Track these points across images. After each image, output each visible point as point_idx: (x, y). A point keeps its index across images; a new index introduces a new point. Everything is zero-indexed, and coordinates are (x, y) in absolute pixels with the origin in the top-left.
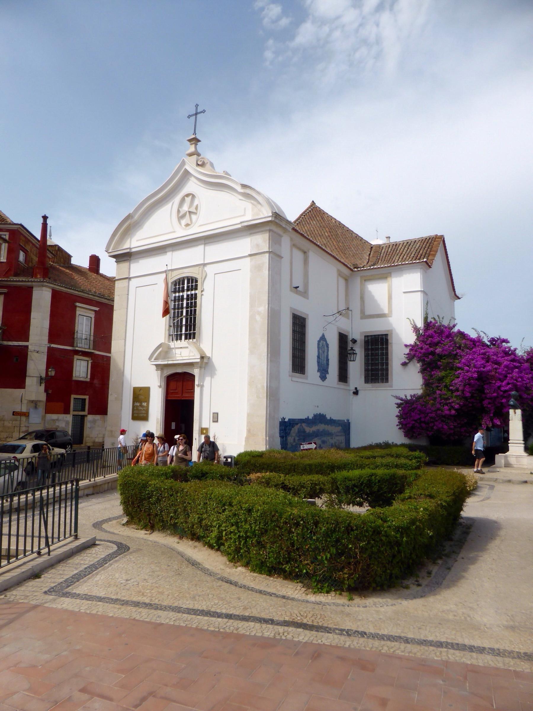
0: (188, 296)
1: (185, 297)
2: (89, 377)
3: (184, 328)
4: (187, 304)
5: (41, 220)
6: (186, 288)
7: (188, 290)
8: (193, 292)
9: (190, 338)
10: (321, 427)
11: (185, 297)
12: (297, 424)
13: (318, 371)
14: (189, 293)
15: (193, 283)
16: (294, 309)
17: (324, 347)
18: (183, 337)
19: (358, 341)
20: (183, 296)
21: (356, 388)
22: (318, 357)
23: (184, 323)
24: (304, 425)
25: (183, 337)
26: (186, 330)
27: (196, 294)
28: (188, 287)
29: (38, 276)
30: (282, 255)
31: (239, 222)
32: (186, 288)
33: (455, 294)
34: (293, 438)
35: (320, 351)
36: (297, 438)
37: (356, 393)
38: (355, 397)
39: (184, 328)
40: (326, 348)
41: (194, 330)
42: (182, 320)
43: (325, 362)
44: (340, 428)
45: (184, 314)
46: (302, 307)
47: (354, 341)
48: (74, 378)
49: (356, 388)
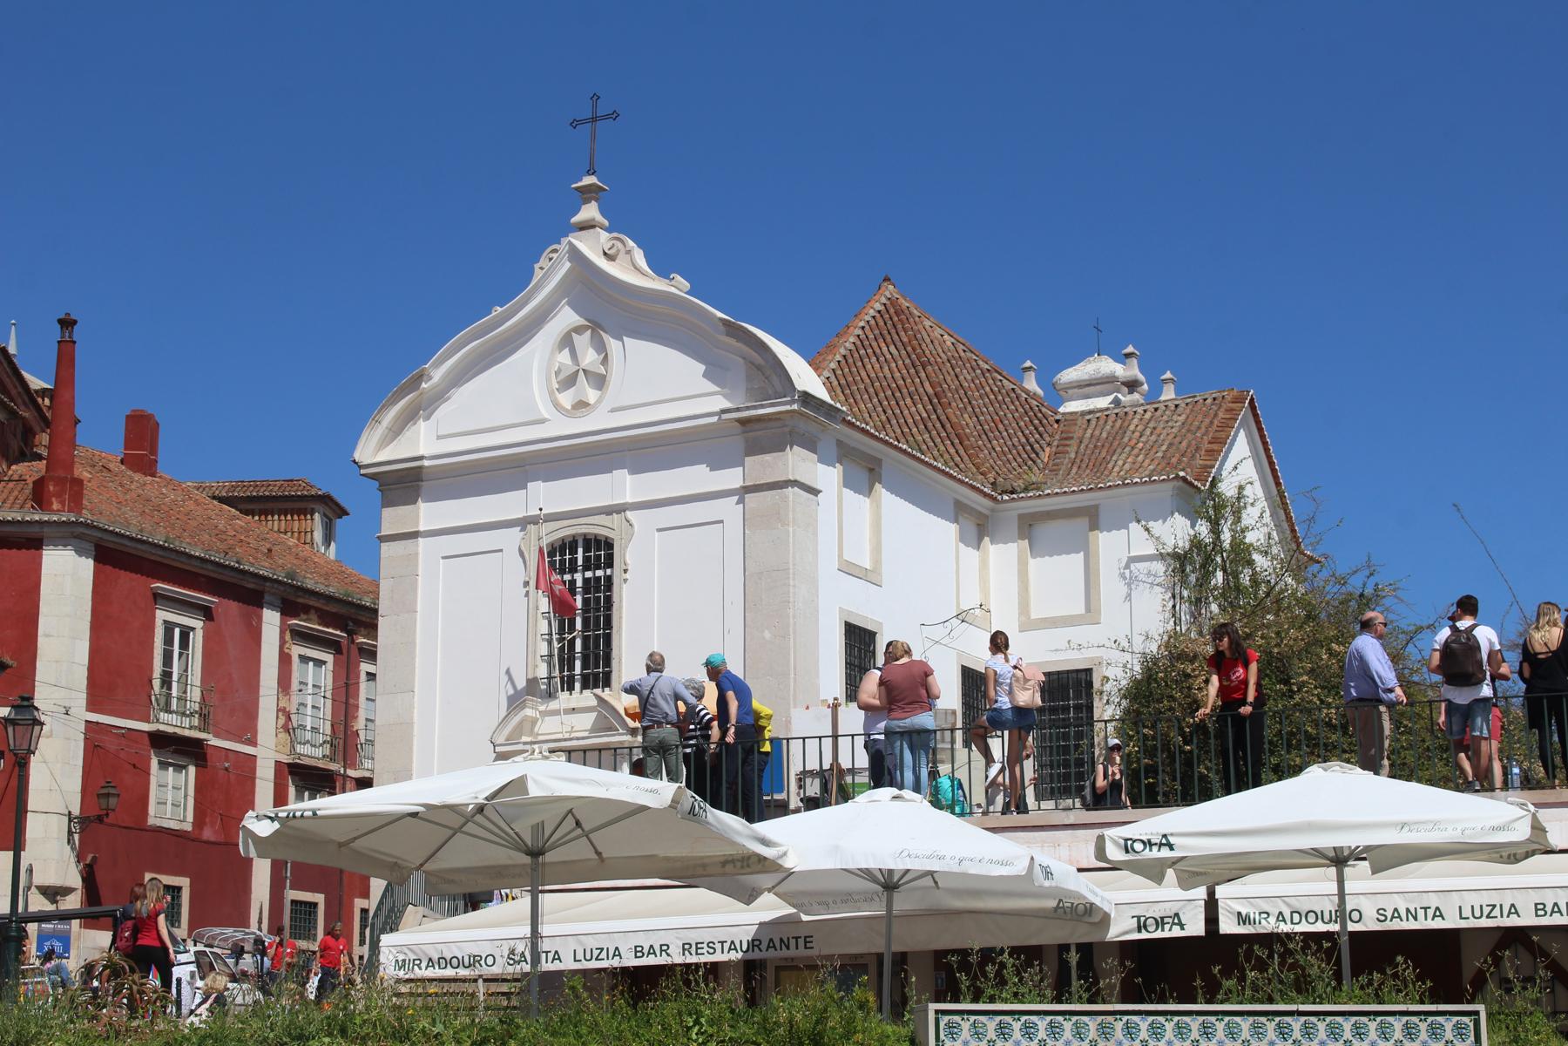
0: (586, 581)
1: (579, 583)
2: (190, 818)
3: (578, 664)
4: (586, 602)
5: (56, 332)
6: (580, 562)
7: (586, 568)
8: (599, 573)
9: (596, 686)
11: (579, 583)
14: (589, 574)
15: (600, 550)
16: (850, 613)
18: (577, 685)
20: (573, 582)
23: (578, 647)
25: (577, 685)
26: (585, 666)
27: (609, 579)
28: (586, 559)
29: (55, 506)
30: (819, 487)
31: (717, 409)
32: (580, 562)
39: (578, 664)
41: (608, 662)
42: (572, 642)
45: (579, 626)
48: (151, 821)
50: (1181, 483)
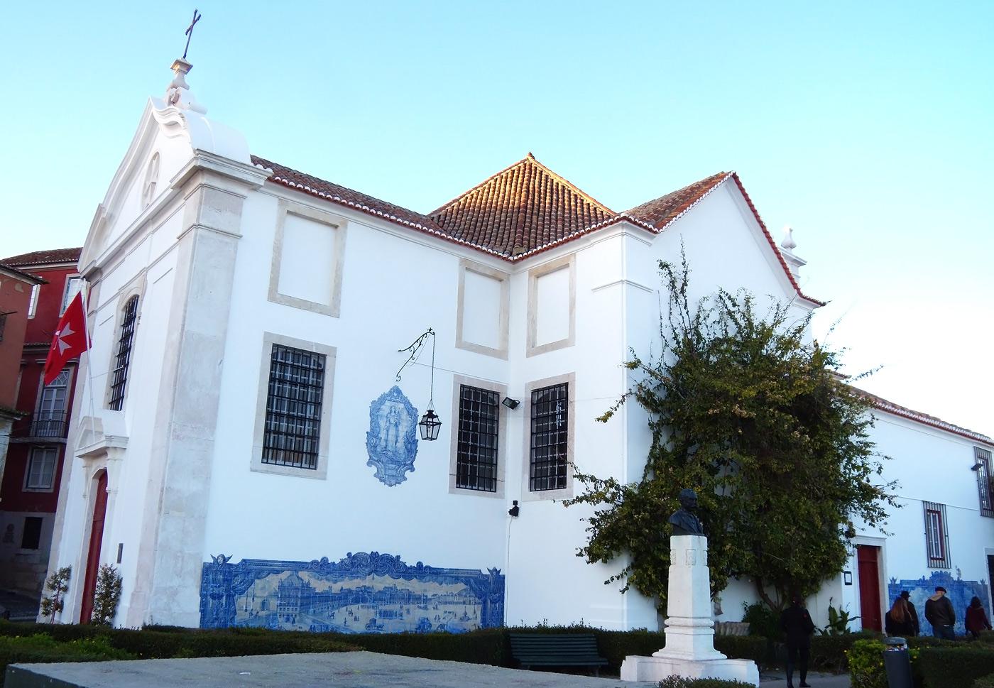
10: (380, 583)
12: (278, 572)
13: (370, 463)
17: (399, 414)
19: (522, 405)
21: (515, 503)
22: (373, 435)
24: (305, 575)
30: (241, 234)
33: (800, 294)
34: (258, 601)
35: (382, 423)
36: (274, 603)
37: (515, 512)
38: (515, 520)
40: (404, 416)
43: (401, 444)
44: (461, 586)
46: (304, 332)
47: (514, 404)
49: (515, 503)
50: (625, 222)
